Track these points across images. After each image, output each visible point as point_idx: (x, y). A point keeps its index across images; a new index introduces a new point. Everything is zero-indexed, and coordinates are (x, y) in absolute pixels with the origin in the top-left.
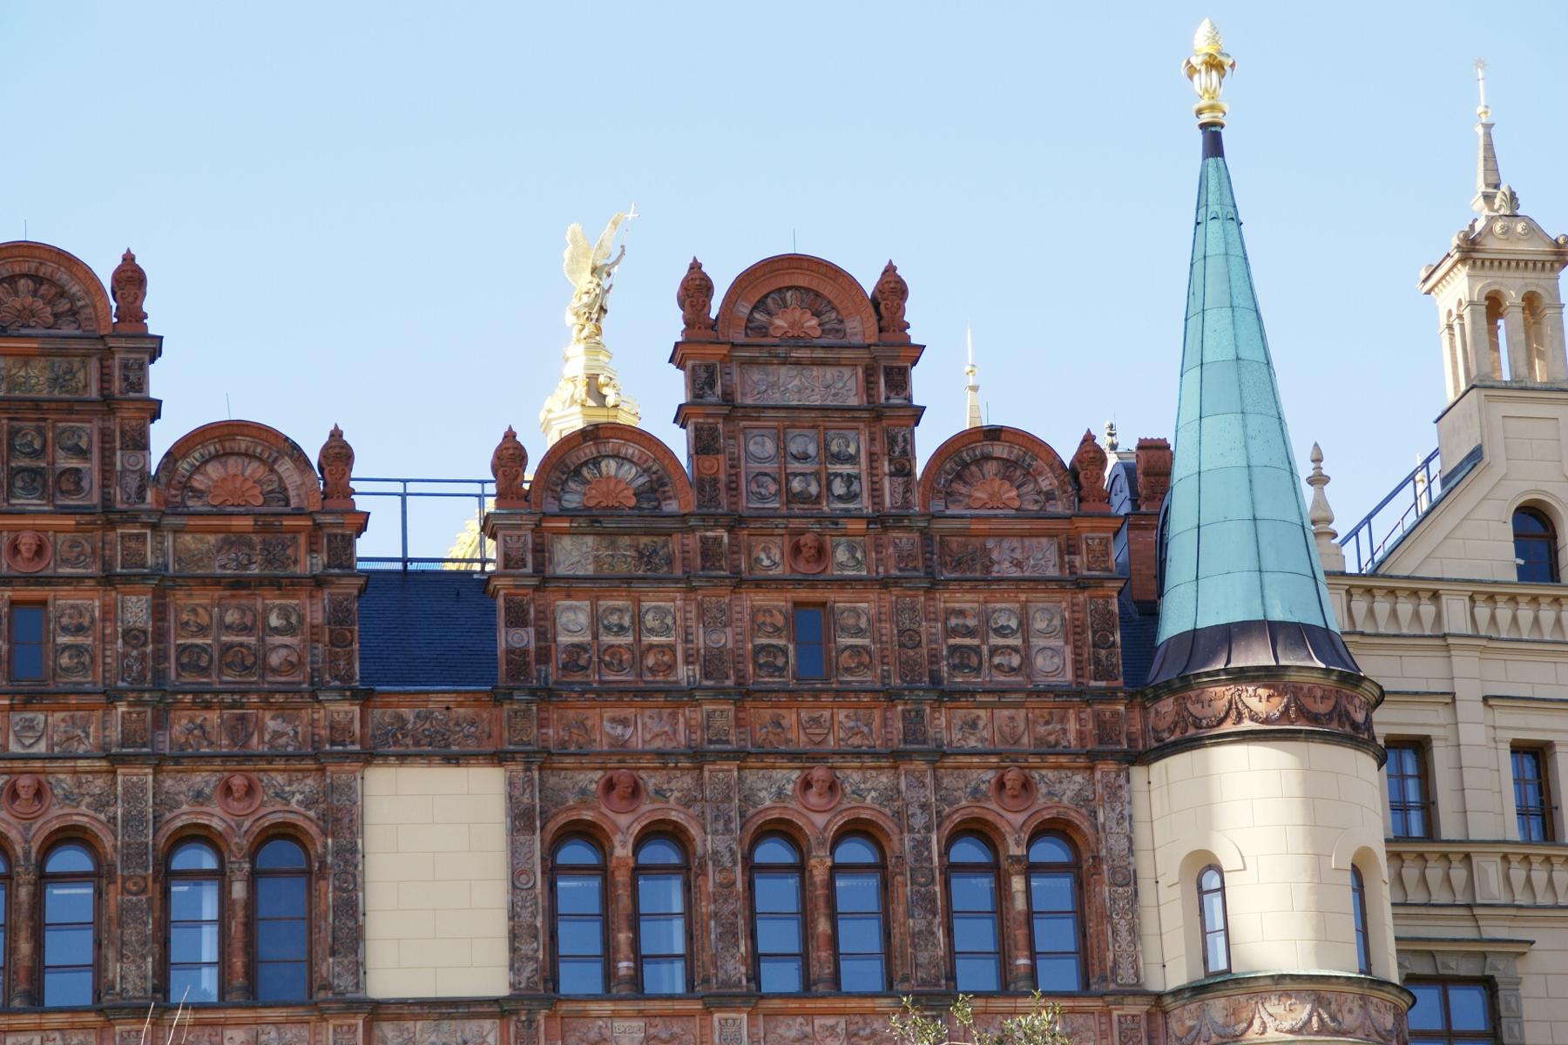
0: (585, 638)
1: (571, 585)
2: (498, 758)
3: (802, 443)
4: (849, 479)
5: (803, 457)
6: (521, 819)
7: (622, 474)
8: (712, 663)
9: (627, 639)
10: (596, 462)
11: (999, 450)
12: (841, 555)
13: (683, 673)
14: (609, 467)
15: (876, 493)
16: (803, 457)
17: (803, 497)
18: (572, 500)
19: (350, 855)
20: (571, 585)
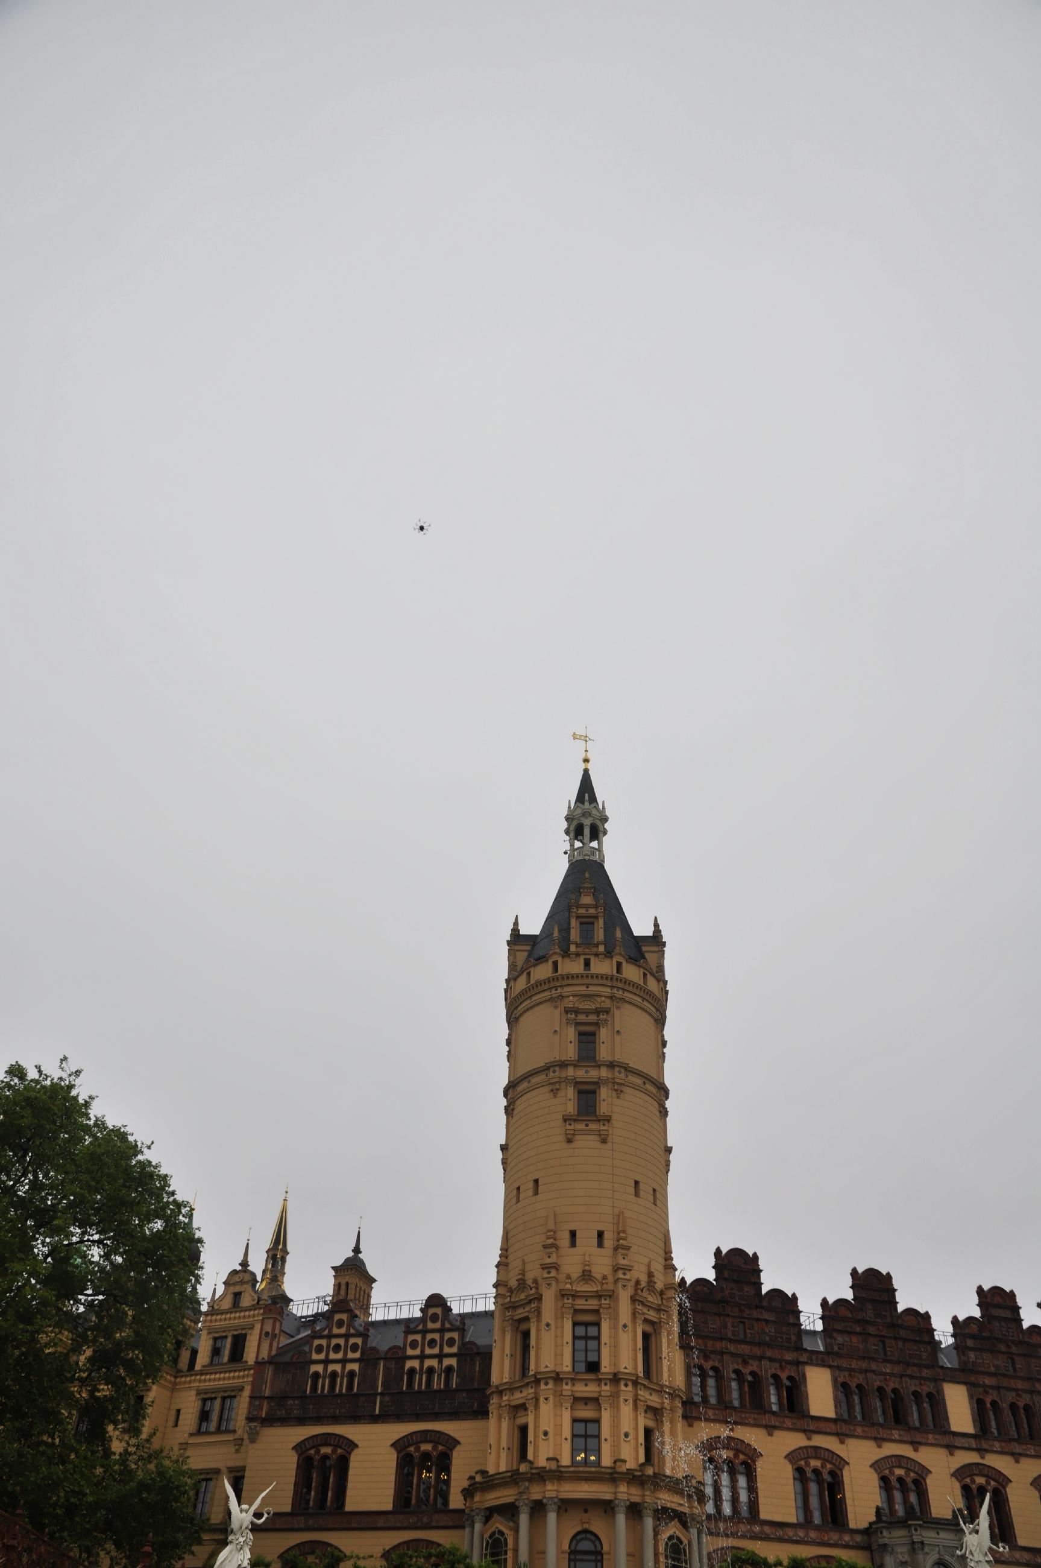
0: (974, 1360)
1: (971, 1349)
2: (965, 1383)
3: (1003, 1324)
4: (1013, 1333)
5: (1004, 1327)
6: (971, 1396)
7: (974, 1328)
8: (997, 1367)
9: (981, 1361)
10: (969, 1324)
11: (1036, 1330)
12: (1014, 1348)
13: (993, 1369)
14: (973, 1325)
15: (1018, 1336)
16: (1004, 1327)
17: (1006, 1335)
18: (967, 1331)
19: (944, 1400)
20: (971, 1349)
